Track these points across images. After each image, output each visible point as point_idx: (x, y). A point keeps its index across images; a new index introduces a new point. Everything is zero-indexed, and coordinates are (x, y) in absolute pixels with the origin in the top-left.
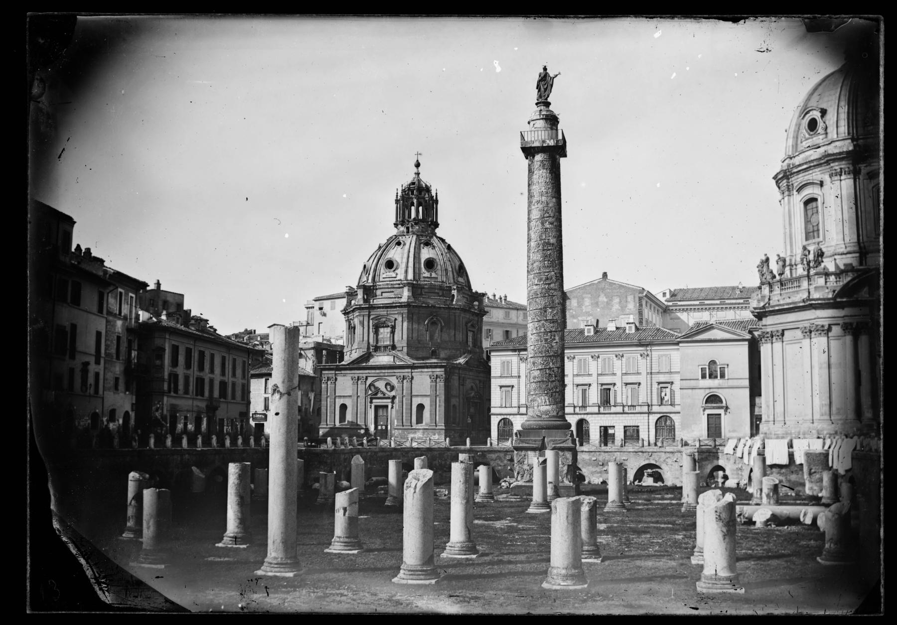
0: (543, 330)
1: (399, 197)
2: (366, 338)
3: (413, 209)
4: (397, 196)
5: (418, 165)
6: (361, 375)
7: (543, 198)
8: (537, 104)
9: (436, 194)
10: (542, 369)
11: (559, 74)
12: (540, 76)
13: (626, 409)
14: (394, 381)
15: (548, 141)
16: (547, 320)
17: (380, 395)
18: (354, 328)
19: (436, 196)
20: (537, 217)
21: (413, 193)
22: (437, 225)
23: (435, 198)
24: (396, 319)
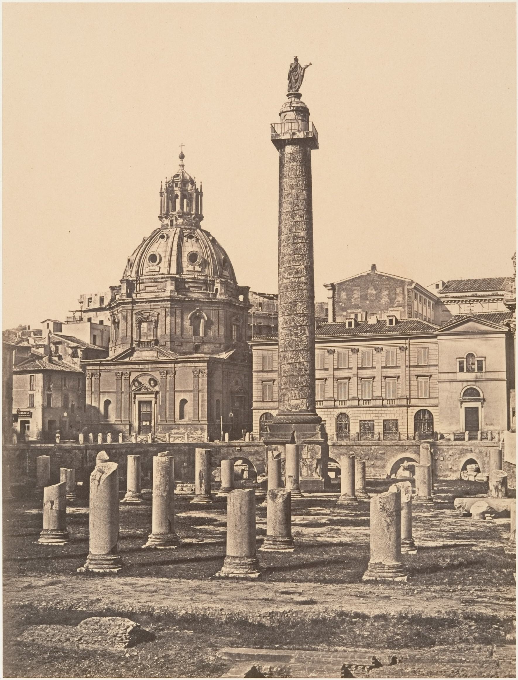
0: (293, 324)
1: (163, 190)
2: (129, 334)
3: (178, 201)
4: (161, 188)
5: (182, 157)
6: (124, 371)
7: (293, 191)
8: (288, 95)
9: (201, 186)
10: (292, 363)
11: (311, 64)
12: (291, 67)
13: (385, 402)
14: (157, 376)
15: (298, 133)
16: (297, 314)
17: (143, 390)
18: (118, 323)
19: (201, 188)
20: (287, 210)
21: (177, 185)
22: (201, 218)
23: (199, 190)
24: (159, 314)
